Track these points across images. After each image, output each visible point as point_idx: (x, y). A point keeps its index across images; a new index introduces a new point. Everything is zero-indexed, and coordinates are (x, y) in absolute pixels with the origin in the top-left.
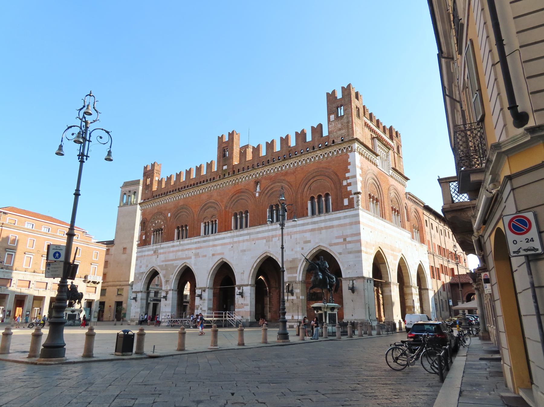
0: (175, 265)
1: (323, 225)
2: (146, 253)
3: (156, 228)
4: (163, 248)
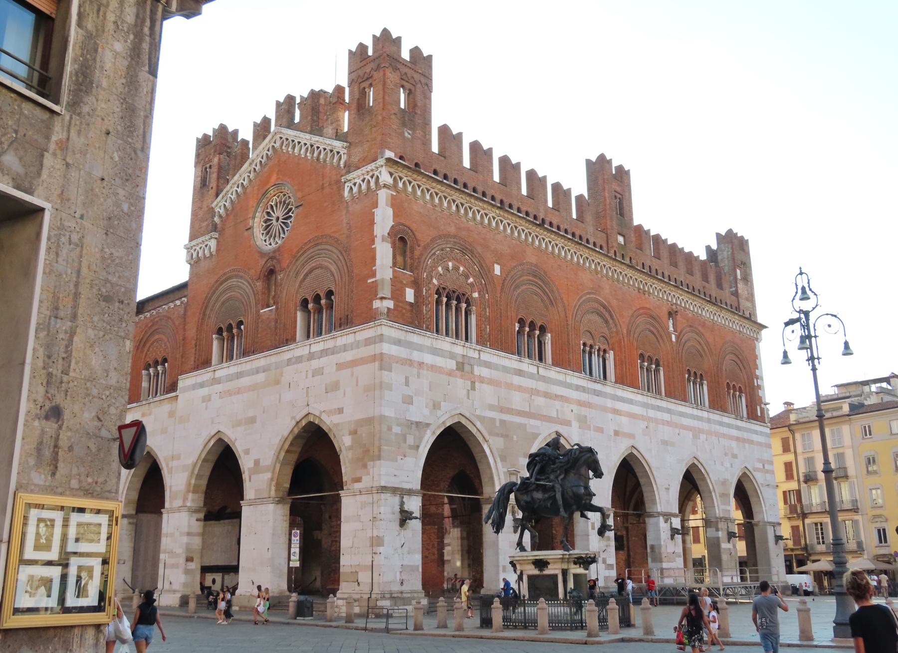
0: (529, 430)
1: (746, 435)
2: (428, 359)
3: (450, 286)
4: (487, 365)
